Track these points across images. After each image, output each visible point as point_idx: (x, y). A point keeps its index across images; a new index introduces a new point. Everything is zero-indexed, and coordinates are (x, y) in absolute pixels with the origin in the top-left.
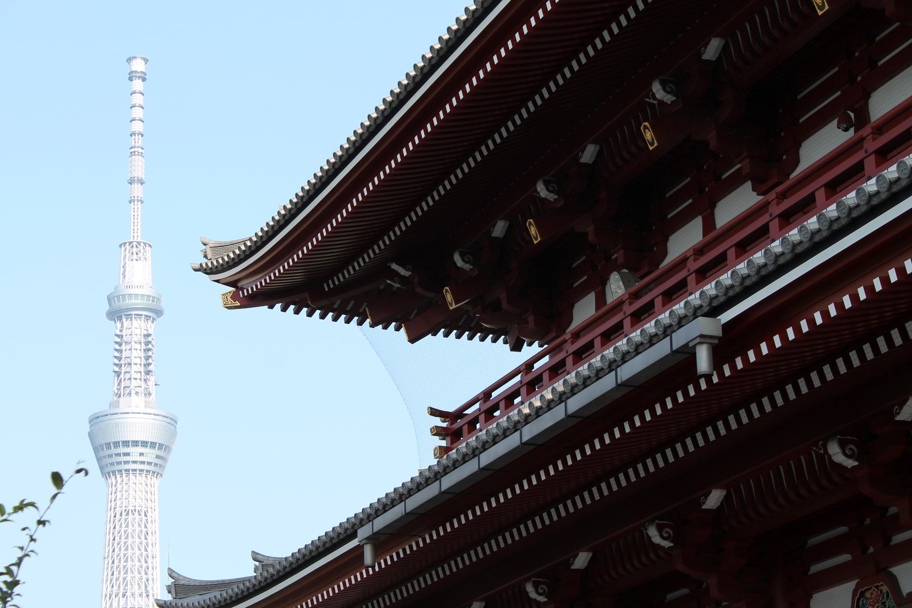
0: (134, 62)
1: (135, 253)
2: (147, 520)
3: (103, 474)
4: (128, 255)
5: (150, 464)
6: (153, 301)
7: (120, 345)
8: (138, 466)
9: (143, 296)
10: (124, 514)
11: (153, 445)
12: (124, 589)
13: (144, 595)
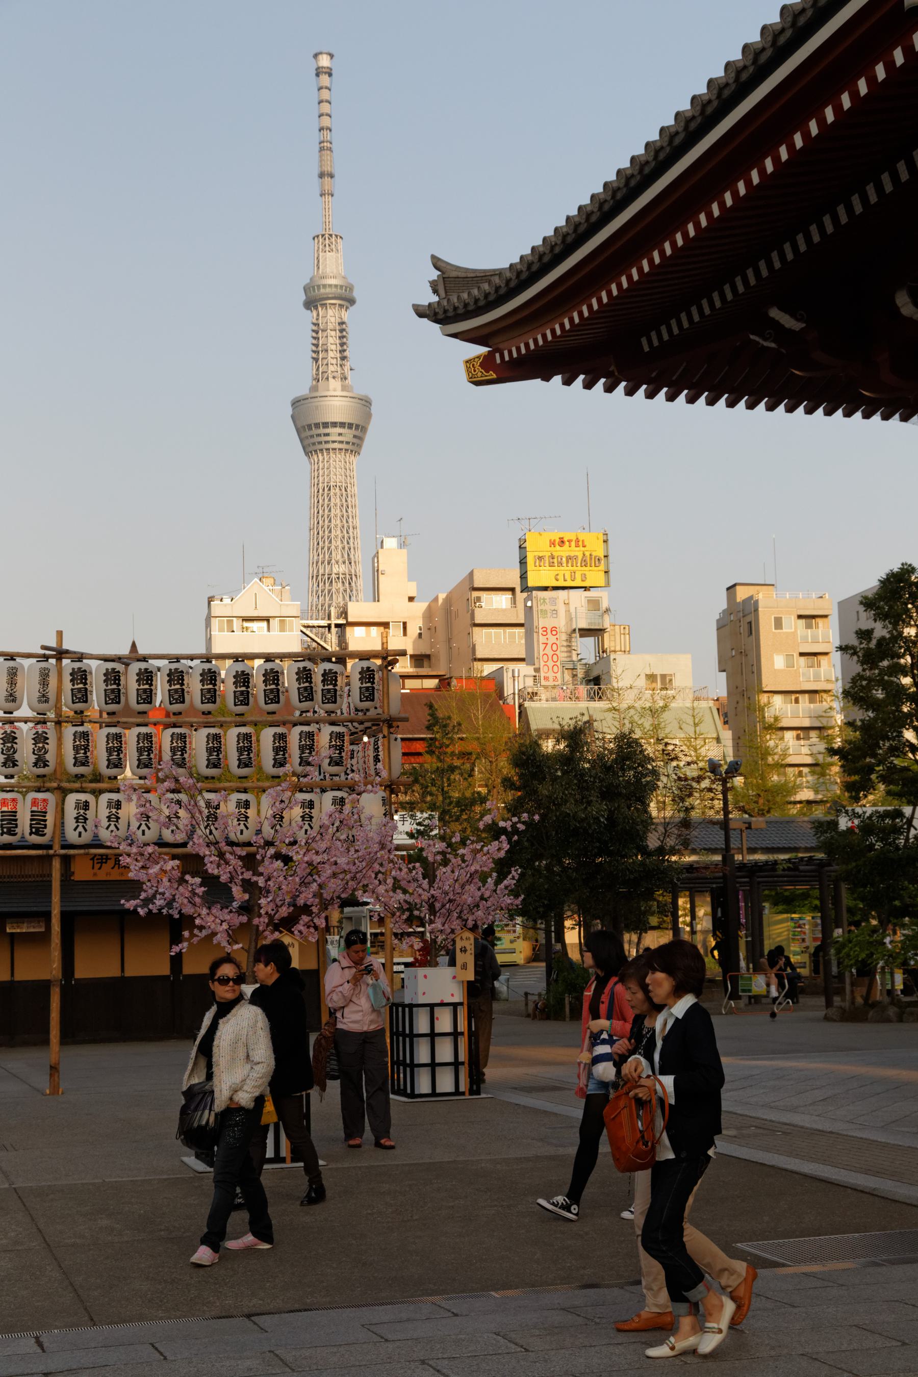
0: (320, 57)
1: (327, 245)
3: (307, 454)
4: (321, 247)
5: (348, 443)
6: (346, 290)
7: (317, 332)
8: (336, 445)
9: (336, 286)
10: (326, 489)
11: (350, 426)
12: (329, 557)
13: (347, 562)
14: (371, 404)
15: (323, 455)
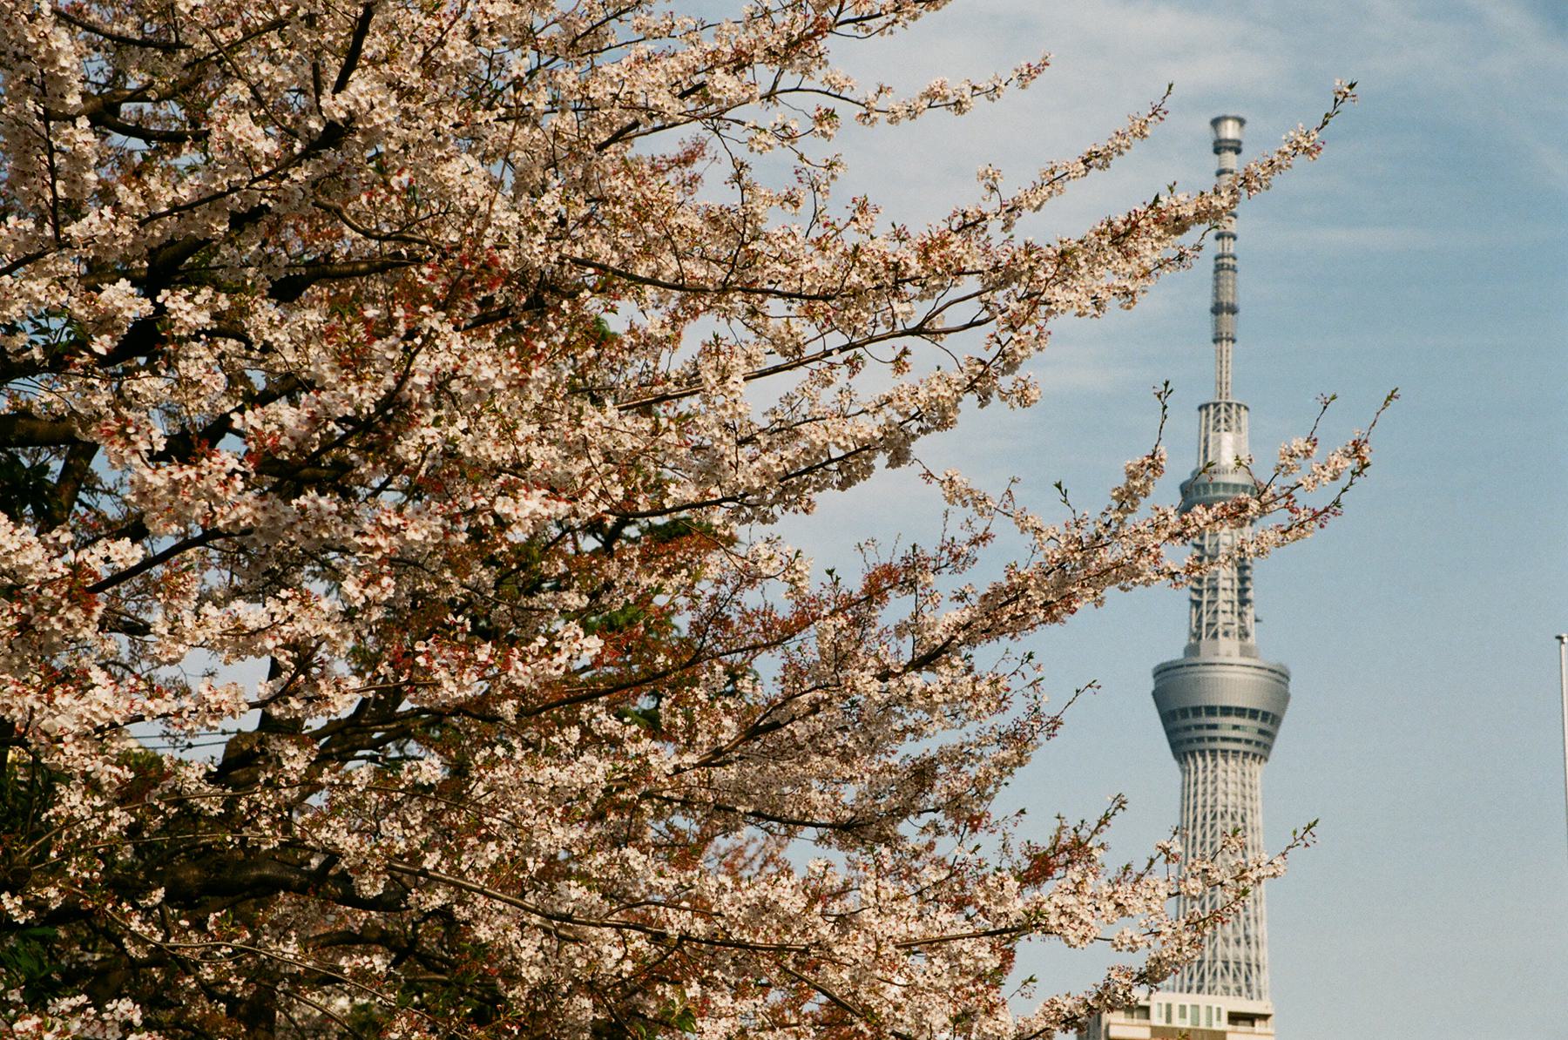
5: (1248, 742)
10: (1209, 817)
11: (1254, 714)
13: (1243, 941)
14: (1288, 678)
15: (1204, 759)
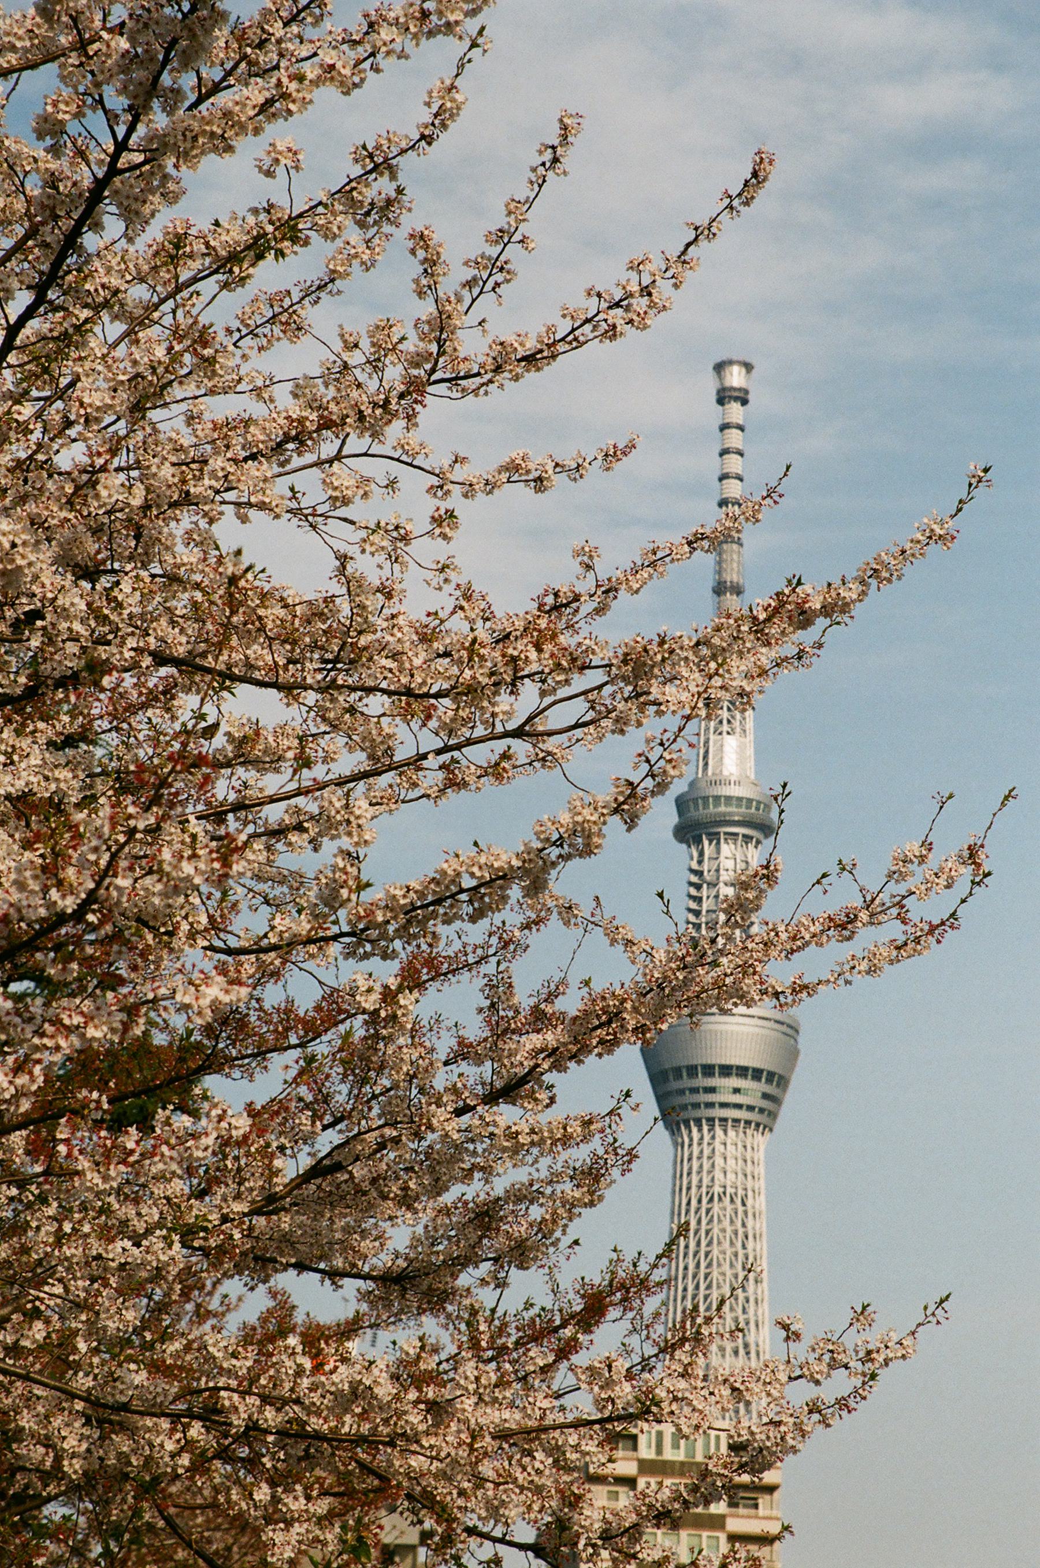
0: (727, 370)
1: (725, 722)
2: (746, 1213)
5: (750, 1108)
6: (757, 809)
7: (698, 887)
10: (705, 1200)
11: (757, 1074)
13: (742, 1352)
14: (797, 1031)
15: (700, 1130)
